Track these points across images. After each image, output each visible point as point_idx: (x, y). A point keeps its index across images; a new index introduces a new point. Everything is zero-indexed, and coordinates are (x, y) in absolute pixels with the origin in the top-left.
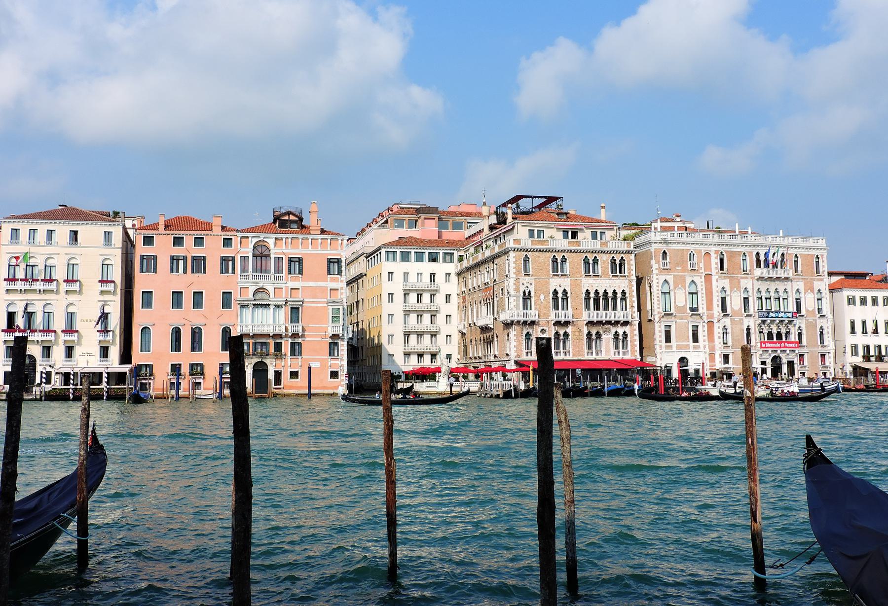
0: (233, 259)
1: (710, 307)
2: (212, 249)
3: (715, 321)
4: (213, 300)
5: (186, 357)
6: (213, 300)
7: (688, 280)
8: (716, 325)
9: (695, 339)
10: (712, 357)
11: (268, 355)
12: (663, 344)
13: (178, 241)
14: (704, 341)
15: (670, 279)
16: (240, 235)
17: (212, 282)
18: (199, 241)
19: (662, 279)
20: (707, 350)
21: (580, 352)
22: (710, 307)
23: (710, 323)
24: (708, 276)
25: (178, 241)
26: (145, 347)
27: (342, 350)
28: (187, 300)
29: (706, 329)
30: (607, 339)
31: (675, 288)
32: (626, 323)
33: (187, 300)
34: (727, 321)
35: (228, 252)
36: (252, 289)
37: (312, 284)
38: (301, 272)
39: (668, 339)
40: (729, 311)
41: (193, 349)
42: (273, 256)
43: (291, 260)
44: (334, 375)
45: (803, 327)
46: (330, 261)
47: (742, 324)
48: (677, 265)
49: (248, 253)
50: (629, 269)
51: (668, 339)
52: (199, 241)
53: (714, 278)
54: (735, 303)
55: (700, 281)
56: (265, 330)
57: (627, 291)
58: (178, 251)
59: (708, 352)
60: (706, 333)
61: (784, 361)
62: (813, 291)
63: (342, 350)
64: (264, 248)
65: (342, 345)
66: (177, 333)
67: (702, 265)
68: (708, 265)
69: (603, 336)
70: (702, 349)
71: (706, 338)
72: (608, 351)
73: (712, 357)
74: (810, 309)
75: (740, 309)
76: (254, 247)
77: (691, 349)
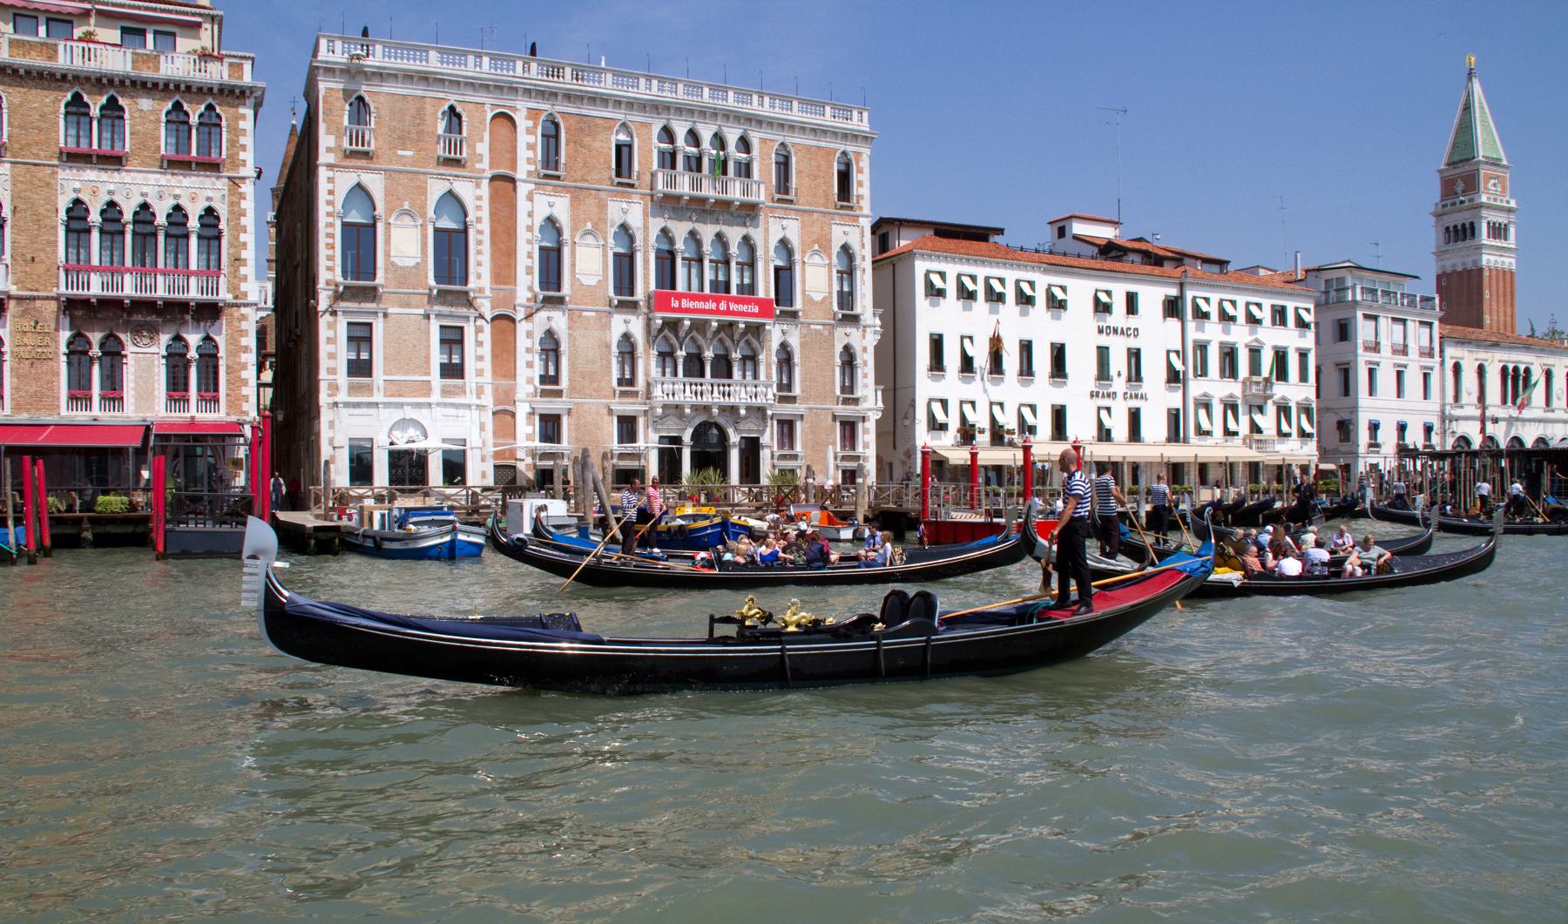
1: (504, 271)
3: (520, 315)
7: (436, 189)
8: (522, 328)
9: (453, 371)
10: (504, 416)
12: (342, 378)
14: (480, 373)
15: (375, 183)
19: (345, 181)
20: (488, 400)
21: (45, 398)
22: (504, 271)
23: (504, 322)
24: (504, 182)
29: (486, 336)
30: (144, 362)
31: (389, 211)
32: (209, 312)
34: (558, 320)
39: (361, 368)
40: (566, 289)
45: (794, 342)
47: (607, 327)
48: (402, 140)
50: (233, 143)
51: (361, 368)
53: (523, 189)
54: (588, 265)
55: (476, 196)
57: (223, 210)
59: (491, 407)
60: (486, 350)
61: (734, 438)
62: (825, 247)
67: (483, 148)
68: (505, 150)
69: (130, 349)
70: (470, 399)
71: (487, 365)
72: (145, 396)
73: (504, 416)
74: (818, 297)
75: (602, 284)
77: (436, 397)
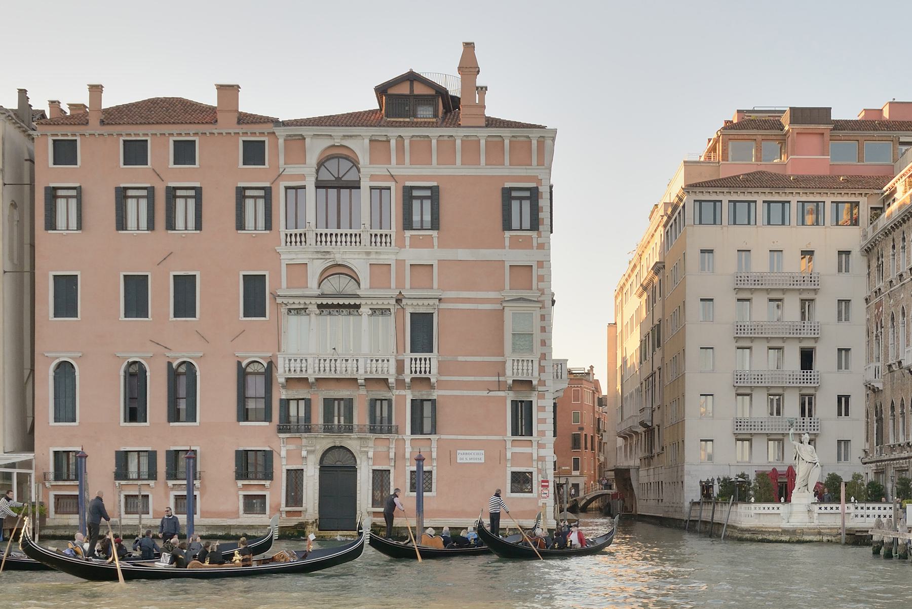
0: (268, 191)
2: (219, 169)
4: (220, 296)
5: (157, 434)
6: (220, 296)
11: (350, 430)
13: (135, 153)
16: (281, 132)
17: (217, 256)
18: (185, 152)
25: (135, 153)
26: (65, 409)
27: (542, 421)
28: (161, 296)
33: (161, 296)
35: (254, 177)
36: (316, 268)
37: (463, 254)
38: (435, 224)
41: (174, 415)
42: (365, 184)
43: (408, 194)
44: (521, 481)
46: (507, 195)
49: (303, 177)
52: (185, 152)
56: (343, 370)
58: (136, 177)
63: (542, 421)
64: (345, 165)
65: (542, 409)
66: (136, 377)
76: (321, 164)
